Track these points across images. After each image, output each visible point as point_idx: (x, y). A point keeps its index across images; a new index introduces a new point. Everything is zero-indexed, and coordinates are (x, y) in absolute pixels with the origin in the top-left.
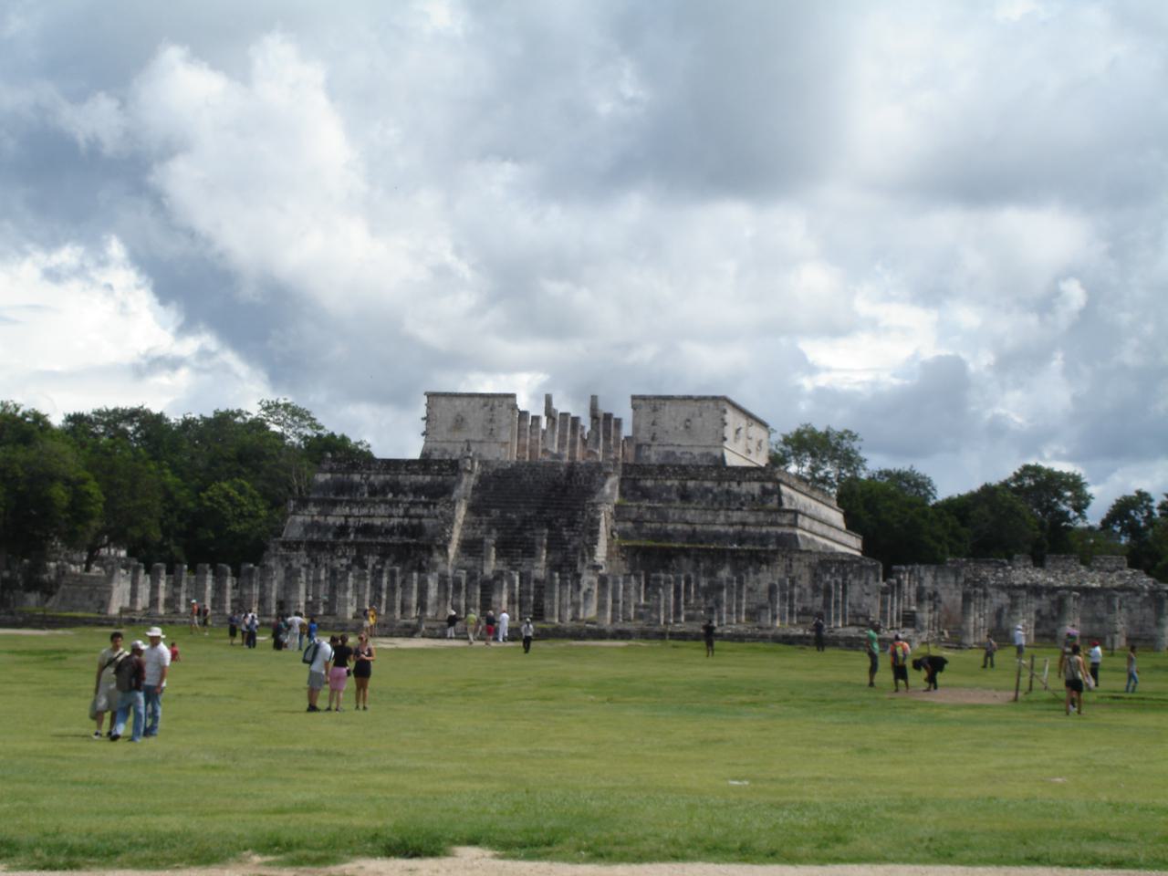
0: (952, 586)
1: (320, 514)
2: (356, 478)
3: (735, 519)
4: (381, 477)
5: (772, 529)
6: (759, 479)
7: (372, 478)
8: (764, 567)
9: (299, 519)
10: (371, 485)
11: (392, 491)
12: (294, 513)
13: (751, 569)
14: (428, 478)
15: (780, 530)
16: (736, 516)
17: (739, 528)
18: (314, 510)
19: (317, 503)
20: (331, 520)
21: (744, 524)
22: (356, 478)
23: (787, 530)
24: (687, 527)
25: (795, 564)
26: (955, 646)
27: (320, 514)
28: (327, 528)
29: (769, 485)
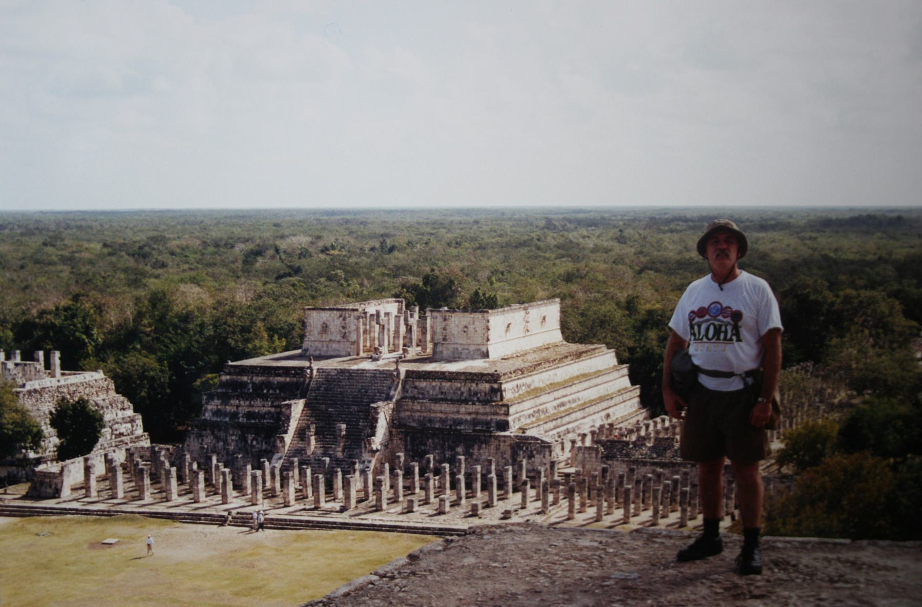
0: (594, 460)
1: (221, 404)
2: (245, 378)
3: (471, 410)
4: (260, 379)
5: (494, 417)
6: (487, 382)
7: (254, 378)
8: (484, 446)
9: (209, 407)
10: (253, 383)
11: (266, 388)
12: (207, 403)
13: (476, 447)
14: (288, 379)
15: (499, 418)
16: (471, 408)
17: (473, 416)
18: (217, 402)
19: (219, 396)
20: (228, 408)
21: (477, 413)
22: (245, 378)
23: (503, 418)
24: (443, 416)
25: (502, 444)
26: (559, 526)
27: (221, 404)
28: (226, 414)
29: (496, 386)
